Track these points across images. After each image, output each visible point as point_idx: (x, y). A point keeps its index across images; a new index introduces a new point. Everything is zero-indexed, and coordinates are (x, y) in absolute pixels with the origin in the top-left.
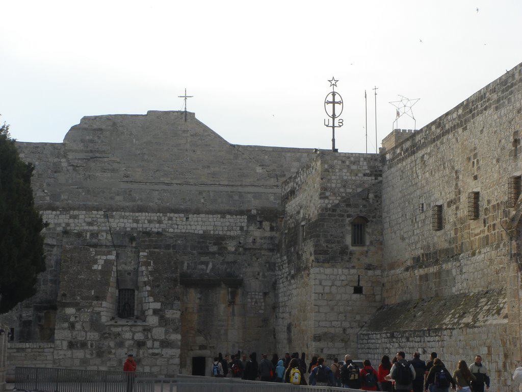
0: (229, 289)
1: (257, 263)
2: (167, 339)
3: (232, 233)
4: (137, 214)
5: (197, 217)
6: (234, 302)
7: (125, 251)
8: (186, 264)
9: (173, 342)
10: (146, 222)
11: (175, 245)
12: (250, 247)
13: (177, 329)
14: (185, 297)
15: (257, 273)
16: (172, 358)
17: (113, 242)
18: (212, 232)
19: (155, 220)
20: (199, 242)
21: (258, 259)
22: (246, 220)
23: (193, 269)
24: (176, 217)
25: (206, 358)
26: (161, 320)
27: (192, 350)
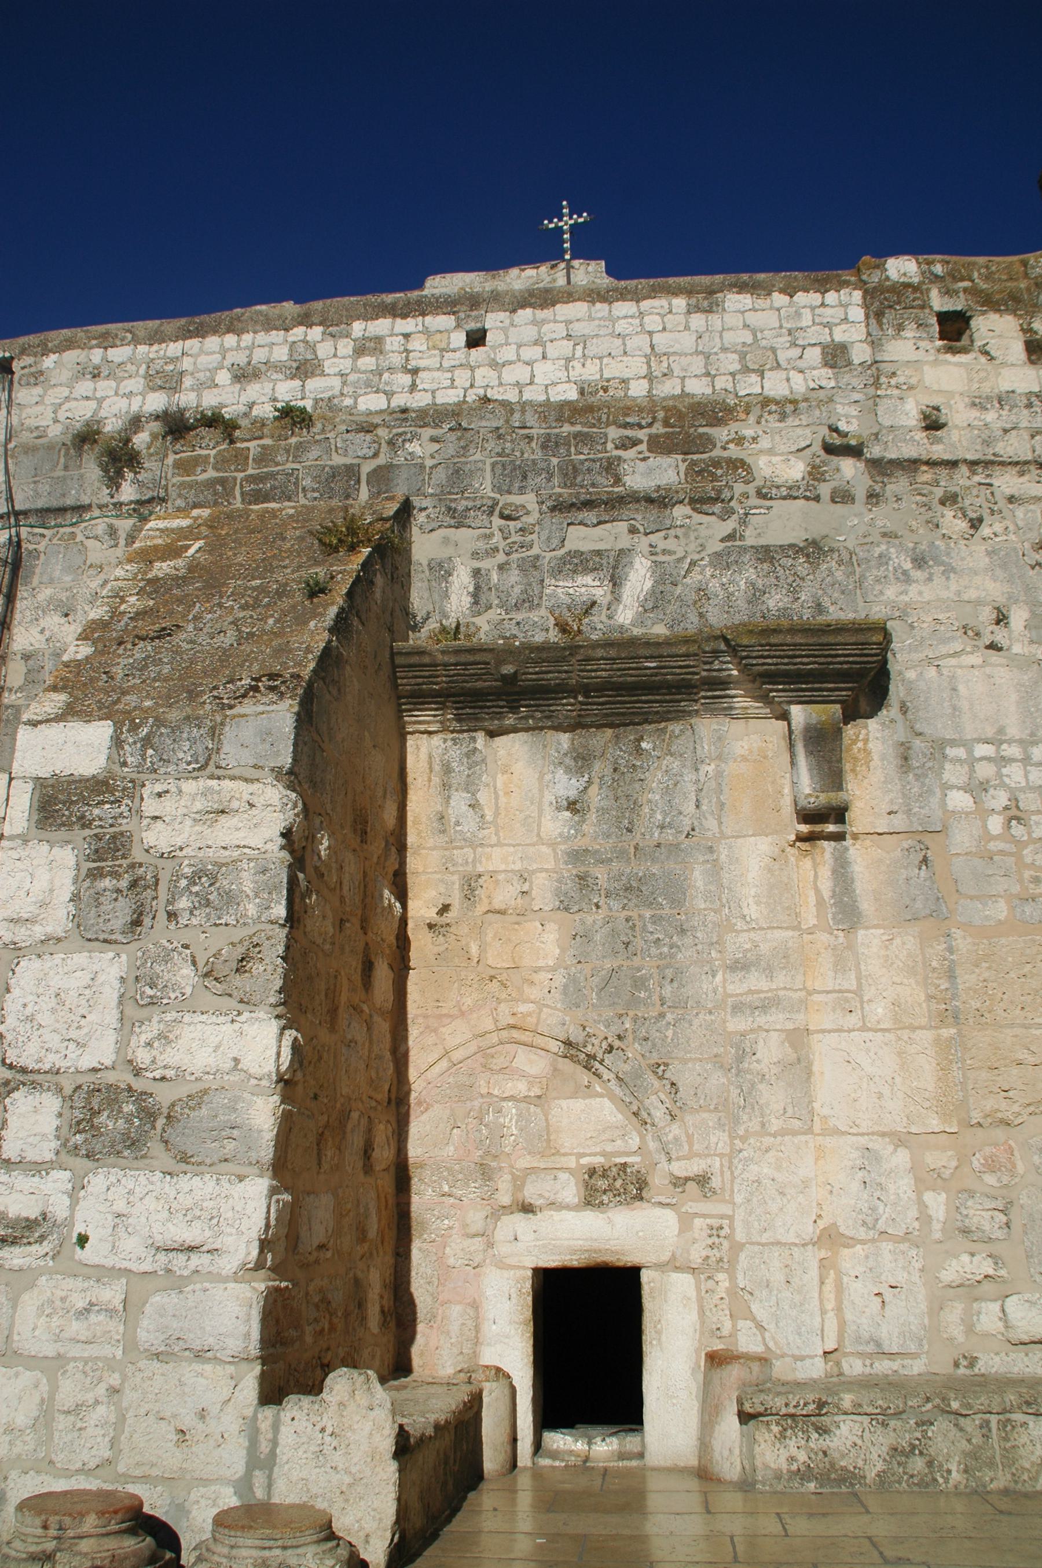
0: (797, 712)
1: (979, 549)
2: (137, 1072)
3: (775, 386)
4: (174, 348)
5: (534, 322)
6: (839, 814)
7: (73, 535)
8: (462, 579)
9: (197, 1099)
10: (223, 377)
11: (389, 467)
12: (909, 452)
13: (242, 965)
14: (459, 801)
15: (987, 614)
16: (175, 1282)
17: (10, 499)
18: (638, 389)
19: (277, 367)
20: (549, 444)
21: (976, 524)
22: (857, 313)
23: (517, 607)
24: (407, 336)
25: (646, 1277)
26: (95, 874)
27: (527, 1209)
